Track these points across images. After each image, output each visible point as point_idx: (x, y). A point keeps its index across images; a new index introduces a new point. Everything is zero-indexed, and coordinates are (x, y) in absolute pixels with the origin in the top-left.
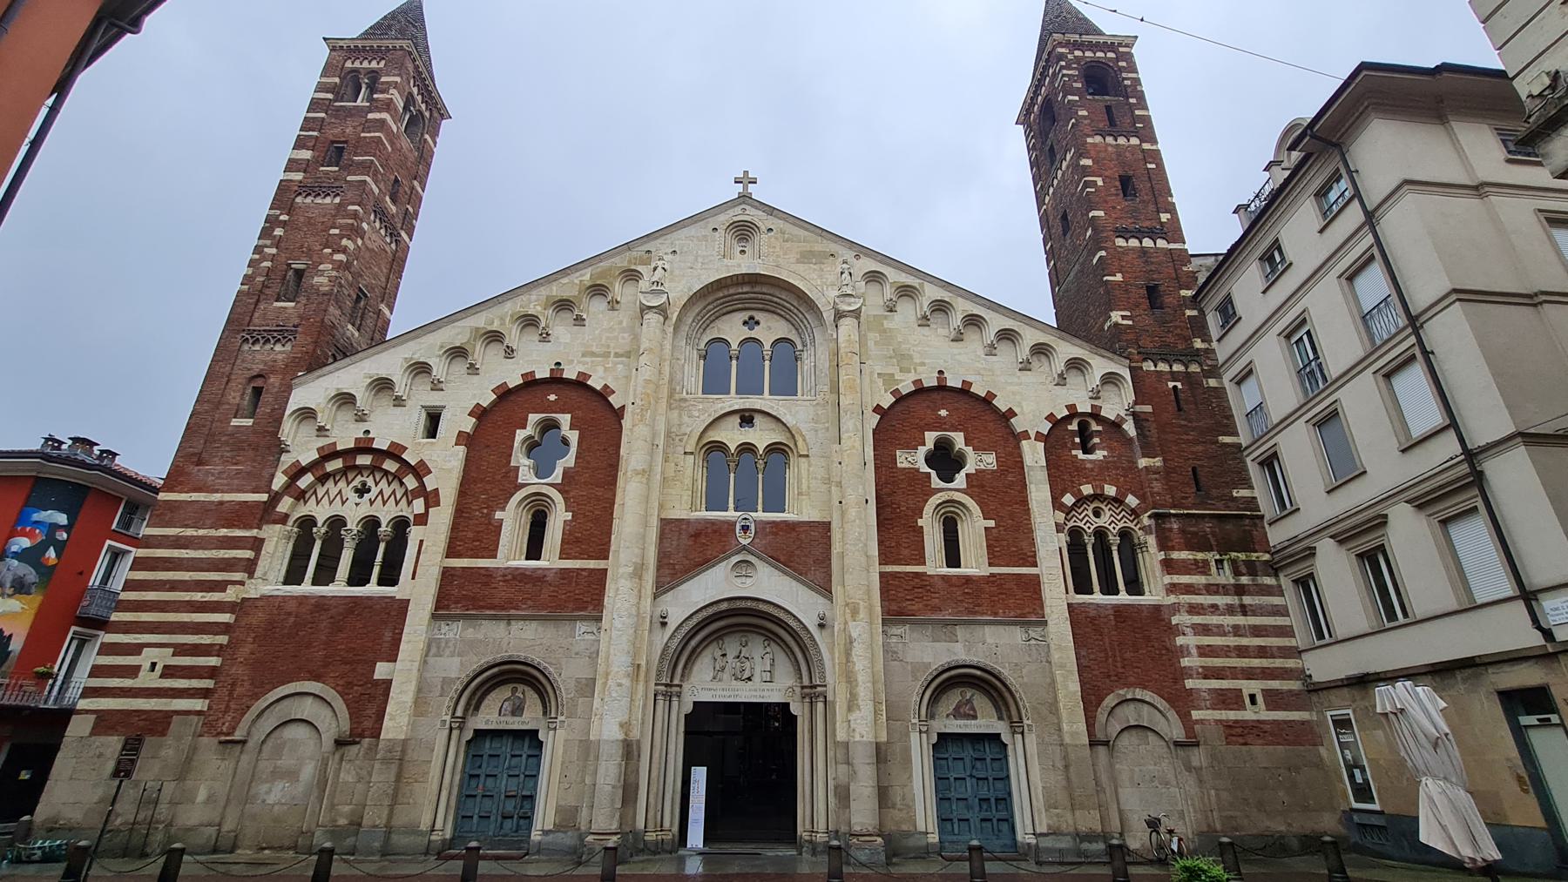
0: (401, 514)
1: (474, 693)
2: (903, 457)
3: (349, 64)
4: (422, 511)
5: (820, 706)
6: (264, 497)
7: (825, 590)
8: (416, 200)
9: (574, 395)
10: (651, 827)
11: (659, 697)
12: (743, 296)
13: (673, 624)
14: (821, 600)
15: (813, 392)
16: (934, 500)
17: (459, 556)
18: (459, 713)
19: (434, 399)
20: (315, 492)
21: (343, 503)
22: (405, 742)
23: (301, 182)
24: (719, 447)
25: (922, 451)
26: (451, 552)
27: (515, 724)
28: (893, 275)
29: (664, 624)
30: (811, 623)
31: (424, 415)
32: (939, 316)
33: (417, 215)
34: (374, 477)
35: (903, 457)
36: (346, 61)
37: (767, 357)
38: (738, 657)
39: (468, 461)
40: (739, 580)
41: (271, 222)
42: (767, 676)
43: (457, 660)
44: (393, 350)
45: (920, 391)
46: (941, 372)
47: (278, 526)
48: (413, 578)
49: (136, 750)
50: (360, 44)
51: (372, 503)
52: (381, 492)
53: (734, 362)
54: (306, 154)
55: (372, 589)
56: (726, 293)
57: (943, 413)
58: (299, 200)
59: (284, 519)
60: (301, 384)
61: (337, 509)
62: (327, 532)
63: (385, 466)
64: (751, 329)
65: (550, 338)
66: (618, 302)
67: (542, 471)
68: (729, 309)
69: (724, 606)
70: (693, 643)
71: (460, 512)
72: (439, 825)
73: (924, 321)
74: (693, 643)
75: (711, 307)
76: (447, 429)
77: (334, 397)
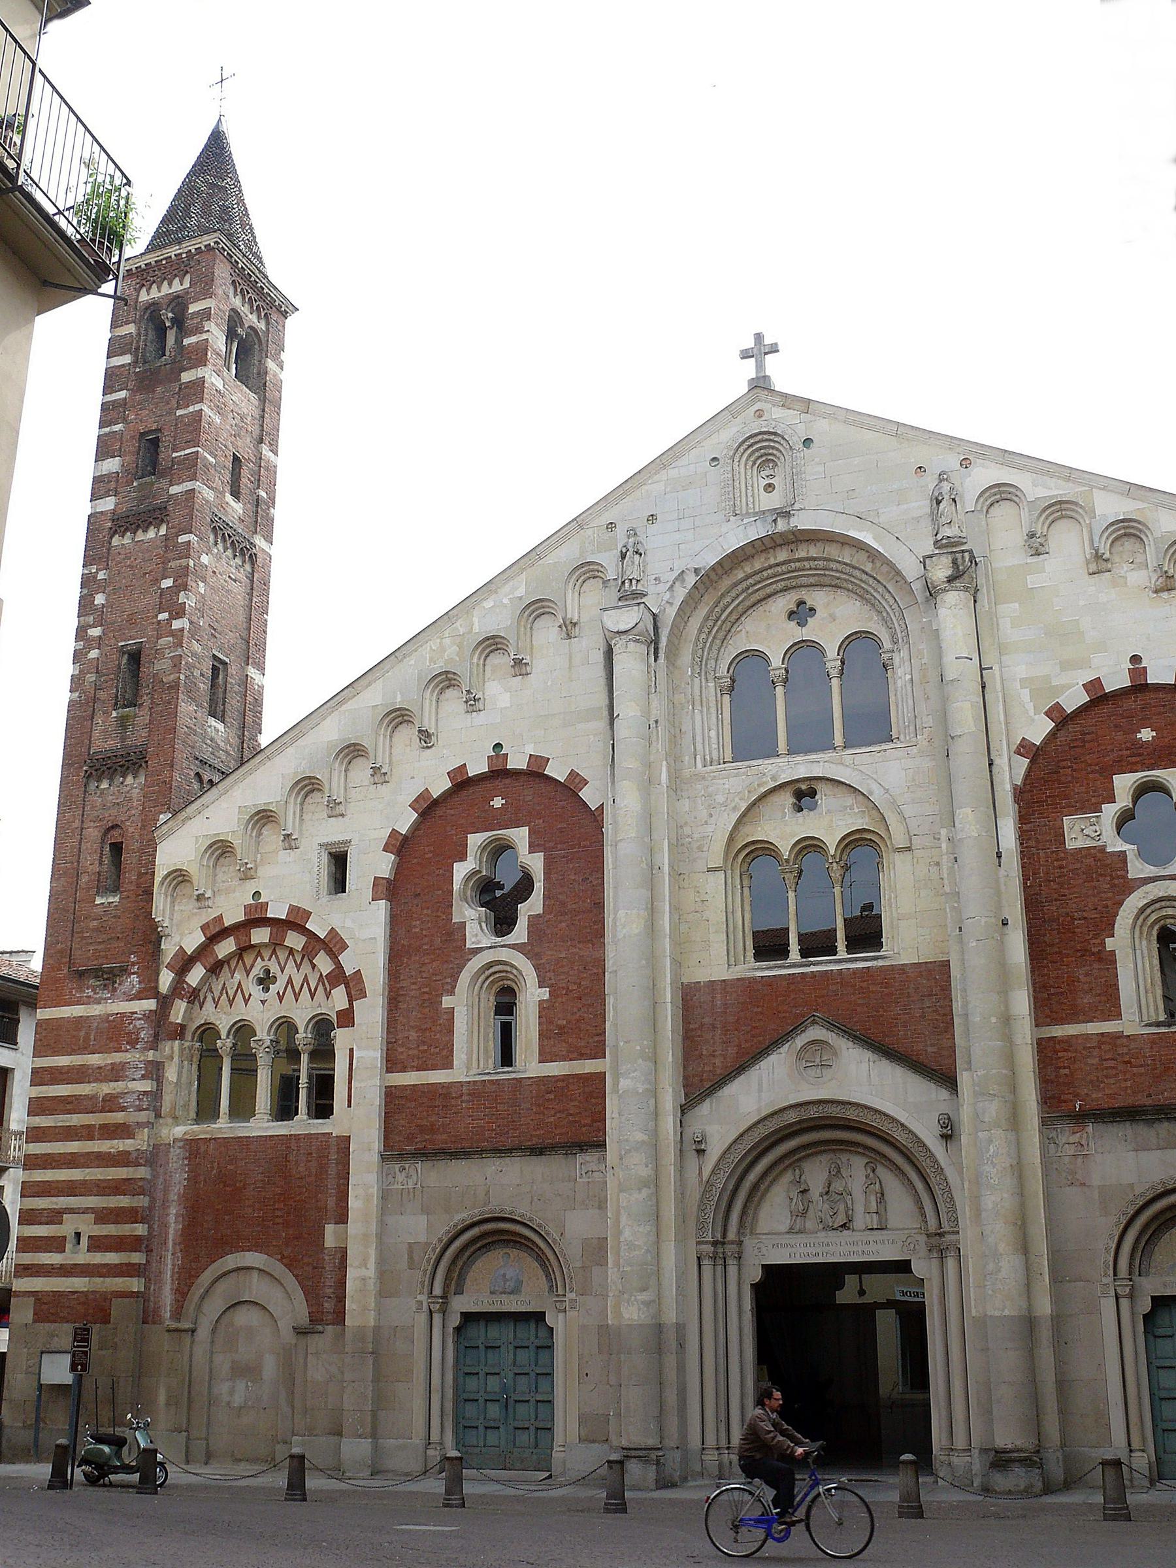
1: (449, 1271)
2: (1077, 828)
3: (144, 297)
4: (345, 1005)
5: (951, 1263)
6: (150, 1004)
7: (948, 1079)
8: (265, 475)
9: (528, 793)
10: (711, 1441)
11: (705, 1262)
12: (779, 569)
13: (714, 1152)
14: (944, 1094)
15: (912, 728)
16: (1134, 902)
17: (404, 1069)
18: (437, 1291)
19: (333, 832)
22: (377, 1329)
23: (114, 512)
24: (762, 850)
25: (1110, 811)
26: (392, 1063)
27: (513, 1305)
28: (1035, 490)
29: (700, 1152)
30: (928, 1133)
31: (325, 858)
32: (1129, 544)
33: (274, 503)
34: (277, 958)
35: (1077, 828)
36: (138, 291)
37: (834, 673)
38: (827, 1193)
39: (395, 921)
40: (812, 1072)
41: (87, 582)
42: (874, 1221)
43: (423, 1219)
44: (269, 764)
45: (1099, 697)
46: (1135, 659)
48: (349, 1106)
49: (86, 1340)
50: (152, 259)
53: (780, 690)
54: (112, 465)
55: (302, 1124)
56: (748, 570)
57: (1146, 735)
58: (116, 541)
59: (179, 1032)
60: (164, 837)
61: (241, 1012)
62: (234, 1045)
63: (288, 943)
64: (802, 624)
65: (480, 705)
66: (575, 624)
67: (503, 923)
68: (761, 594)
69: (792, 1117)
70: (752, 1177)
71: (394, 1001)
72: (435, 1437)
73: (1099, 563)
74: (752, 1177)
75: (729, 599)
76: (360, 875)
77: (206, 851)
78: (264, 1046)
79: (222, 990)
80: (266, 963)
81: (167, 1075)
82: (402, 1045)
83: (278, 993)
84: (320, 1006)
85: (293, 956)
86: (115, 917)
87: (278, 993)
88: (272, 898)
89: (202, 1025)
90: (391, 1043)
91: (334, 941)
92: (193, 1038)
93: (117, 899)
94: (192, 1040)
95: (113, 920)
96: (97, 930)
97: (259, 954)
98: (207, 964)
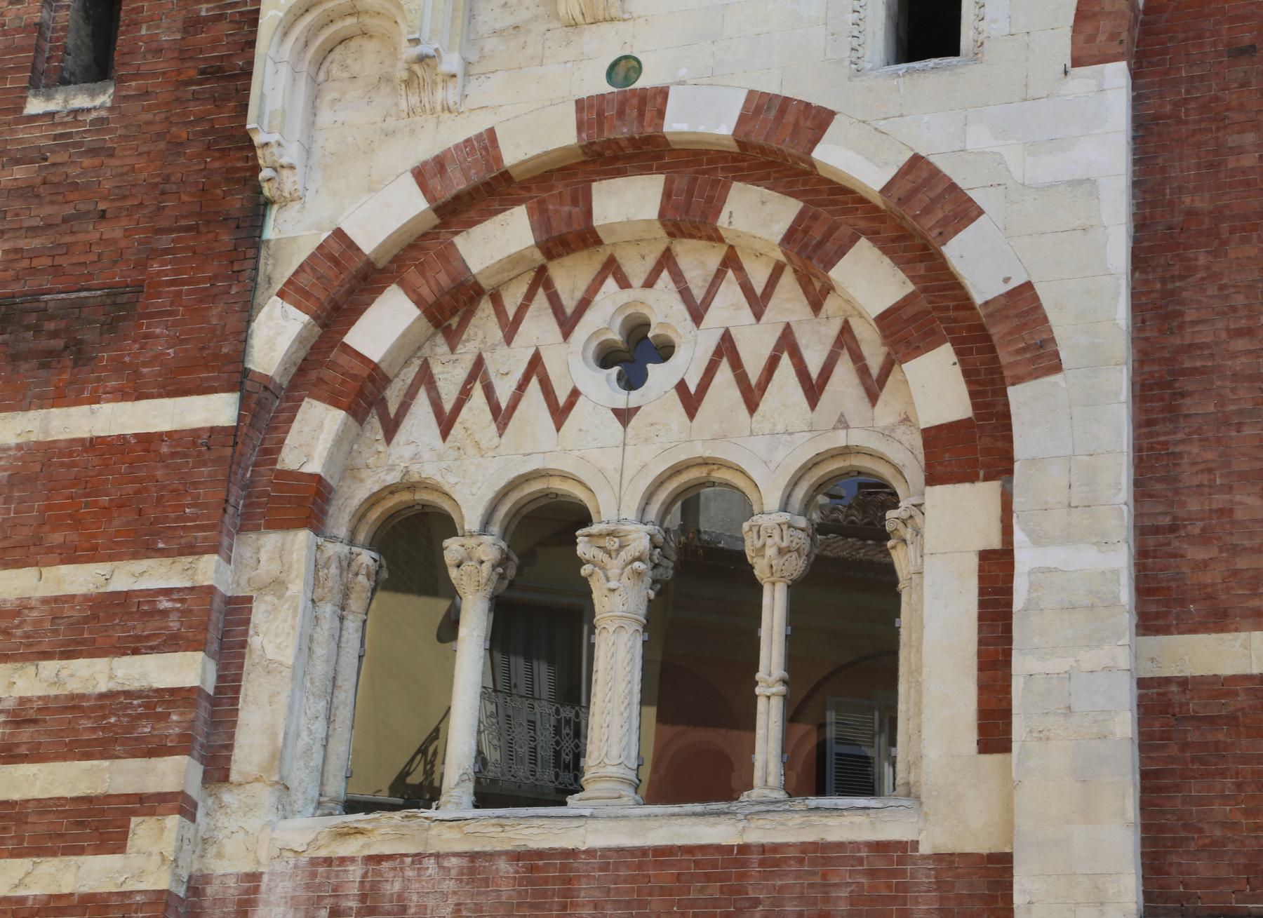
0: (840, 439)
20: (426, 378)
21: (560, 413)
34: (678, 277)
47: (303, 537)
51: (691, 401)
52: (727, 348)
78: (625, 555)
79: (472, 378)
80: (636, 293)
81: (255, 641)
82: (1205, 538)
83: (681, 387)
85: (740, 270)
86: (93, 152)
87: (681, 387)
88: (683, 73)
89: (392, 490)
90: (1156, 530)
92: (353, 533)
93: (104, 98)
94: (351, 542)
95: (87, 162)
96: (27, 192)
97: (612, 268)
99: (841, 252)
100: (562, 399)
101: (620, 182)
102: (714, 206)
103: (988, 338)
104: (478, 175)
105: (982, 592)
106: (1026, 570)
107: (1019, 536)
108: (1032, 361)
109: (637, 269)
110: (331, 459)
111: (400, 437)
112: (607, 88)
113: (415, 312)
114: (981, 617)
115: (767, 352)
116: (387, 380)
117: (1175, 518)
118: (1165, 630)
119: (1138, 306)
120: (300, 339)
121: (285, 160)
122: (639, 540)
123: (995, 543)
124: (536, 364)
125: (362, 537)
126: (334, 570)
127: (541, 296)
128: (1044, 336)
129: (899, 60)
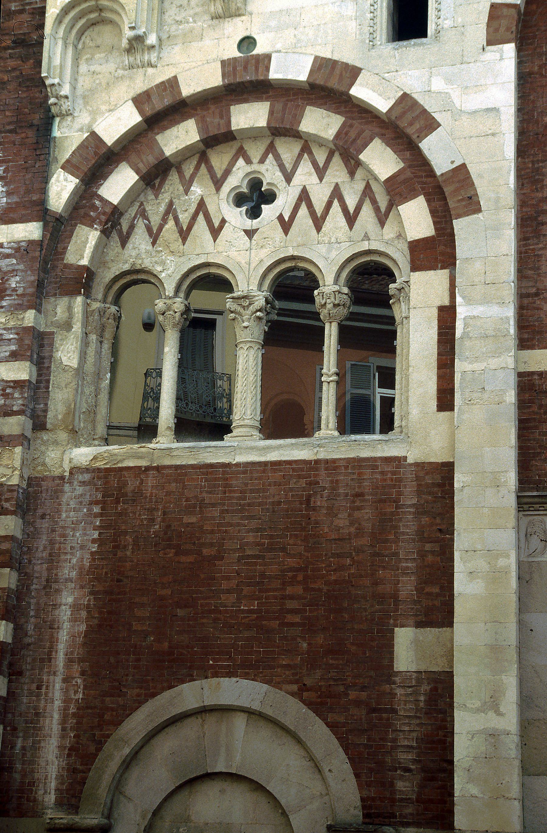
0: (365, 246)
20: (143, 214)
21: (215, 232)
34: (277, 158)
80: (255, 167)
83: (280, 218)
84: (366, 237)
85: (310, 153)
87: (280, 218)
88: (278, 46)
90: (528, 295)
91: (409, 116)
92: (105, 296)
94: (104, 301)
97: (241, 152)
98: (141, 165)
99: (365, 146)
100: (216, 224)
101: (245, 106)
102: (298, 118)
103: (443, 193)
104: (167, 102)
105: (440, 328)
106: (463, 317)
107: (459, 299)
108: (465, 206)
109: (255, 154)
110: (92, 258)
111: (129, 245)
112: (238, 54)
113: (137, 177)
114: (439, 341)
115: (326, 199)
116: (121, 214)
117: (538, 289)
118: (532, 347)
119: (519, 176)
120: (74, 193)
121: (63, 93)
122: (260, 302)
123: (446, 302)
124: (201, 206)
125: (110, 299)
126: (96, 317)
127: (203, 169)
128: (472, 193)
129: (394, 40)
